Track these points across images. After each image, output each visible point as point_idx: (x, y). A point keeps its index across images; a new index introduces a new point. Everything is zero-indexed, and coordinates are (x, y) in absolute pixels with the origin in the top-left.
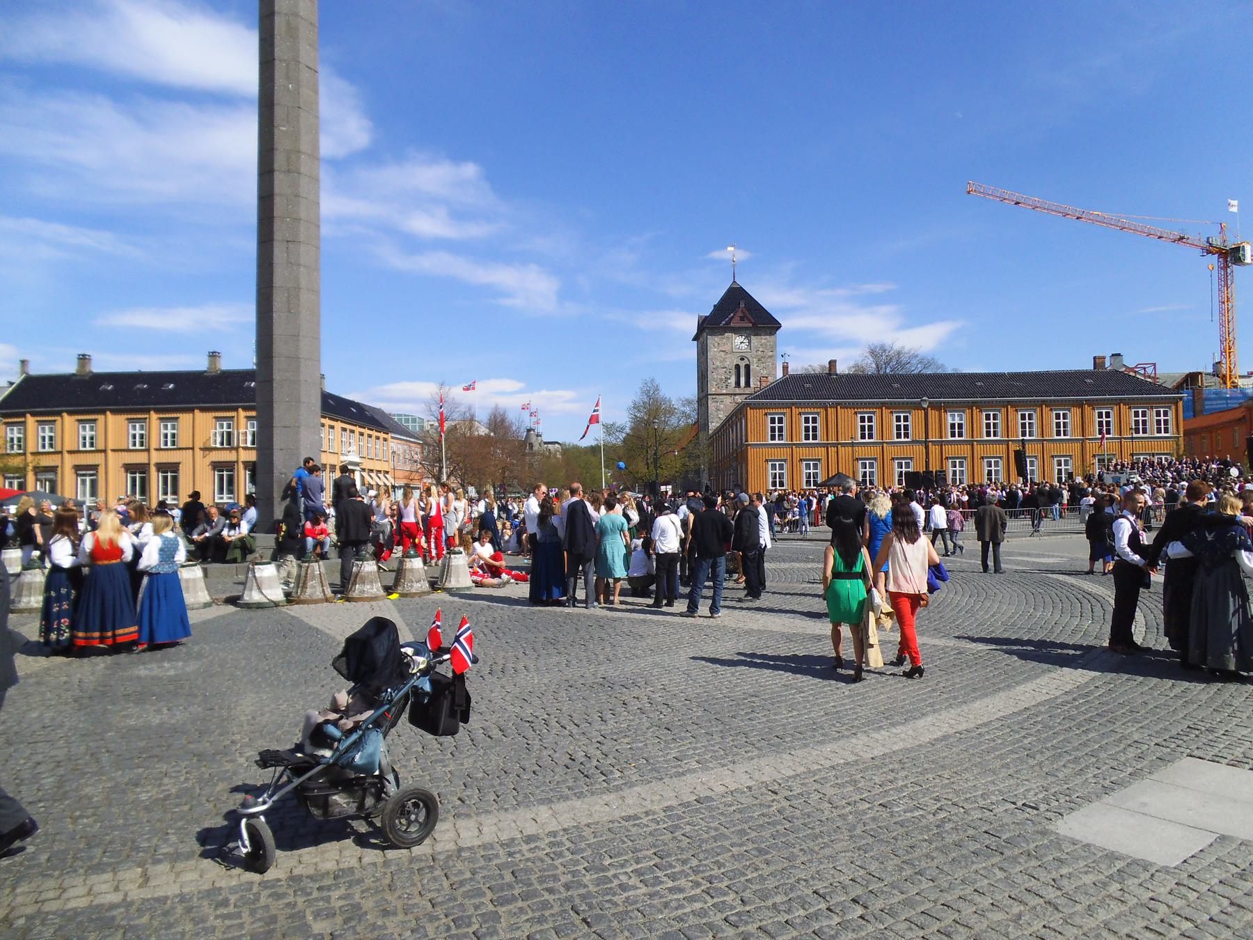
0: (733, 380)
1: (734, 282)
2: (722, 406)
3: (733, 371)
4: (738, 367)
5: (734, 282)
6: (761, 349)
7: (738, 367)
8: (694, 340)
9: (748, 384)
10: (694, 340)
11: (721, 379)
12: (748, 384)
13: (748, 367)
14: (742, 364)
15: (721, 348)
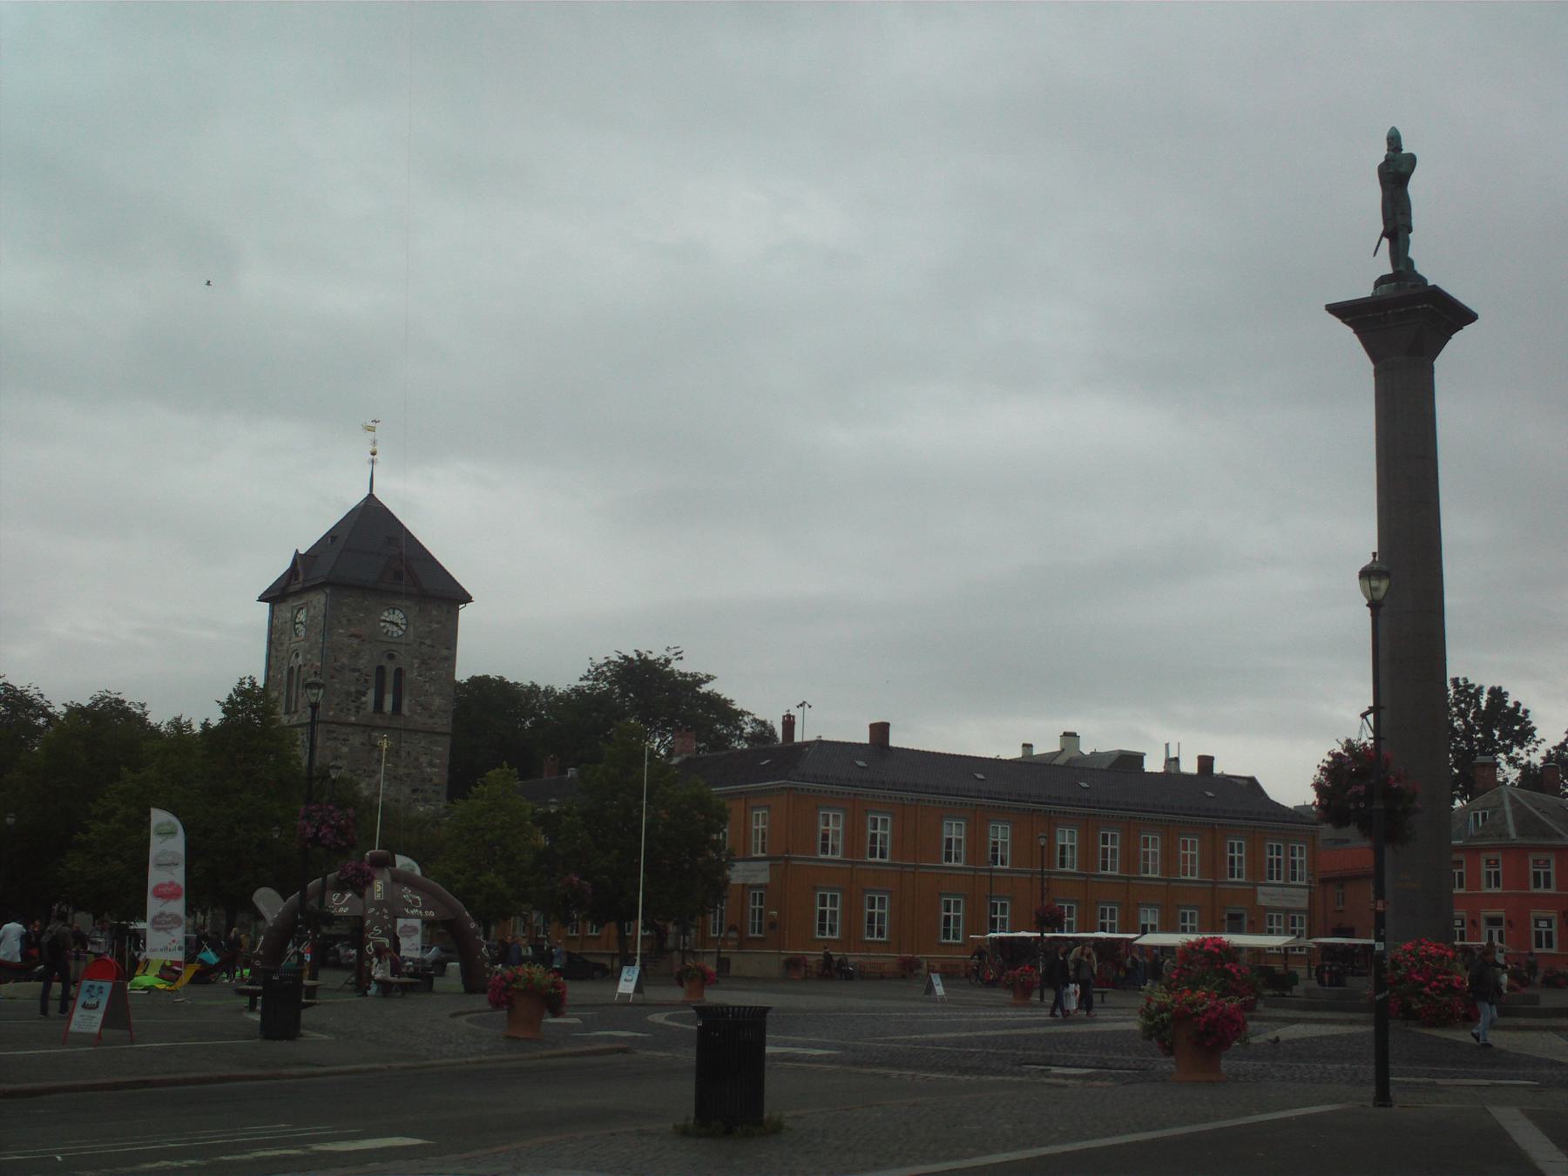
0: (370, 698)
1: (371, 496)
2: (345, 750)
3: (372, 680)
4: (381, 670)
5: (371, 496)
6: (428, 642)
7: (381, 670)
8: (262, 599)
9: (397, 706)
10: (262, 599)
11: (349, 694)
12: (397, 706)
13: (399, 673)
14: (391, 668)
15: (353, 630)
